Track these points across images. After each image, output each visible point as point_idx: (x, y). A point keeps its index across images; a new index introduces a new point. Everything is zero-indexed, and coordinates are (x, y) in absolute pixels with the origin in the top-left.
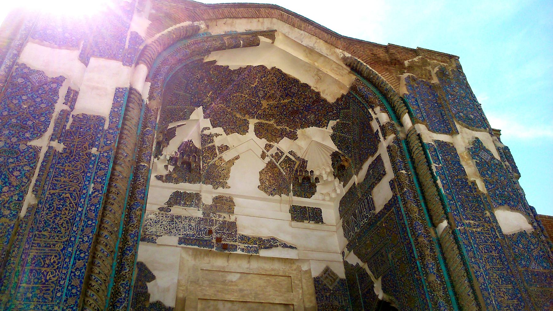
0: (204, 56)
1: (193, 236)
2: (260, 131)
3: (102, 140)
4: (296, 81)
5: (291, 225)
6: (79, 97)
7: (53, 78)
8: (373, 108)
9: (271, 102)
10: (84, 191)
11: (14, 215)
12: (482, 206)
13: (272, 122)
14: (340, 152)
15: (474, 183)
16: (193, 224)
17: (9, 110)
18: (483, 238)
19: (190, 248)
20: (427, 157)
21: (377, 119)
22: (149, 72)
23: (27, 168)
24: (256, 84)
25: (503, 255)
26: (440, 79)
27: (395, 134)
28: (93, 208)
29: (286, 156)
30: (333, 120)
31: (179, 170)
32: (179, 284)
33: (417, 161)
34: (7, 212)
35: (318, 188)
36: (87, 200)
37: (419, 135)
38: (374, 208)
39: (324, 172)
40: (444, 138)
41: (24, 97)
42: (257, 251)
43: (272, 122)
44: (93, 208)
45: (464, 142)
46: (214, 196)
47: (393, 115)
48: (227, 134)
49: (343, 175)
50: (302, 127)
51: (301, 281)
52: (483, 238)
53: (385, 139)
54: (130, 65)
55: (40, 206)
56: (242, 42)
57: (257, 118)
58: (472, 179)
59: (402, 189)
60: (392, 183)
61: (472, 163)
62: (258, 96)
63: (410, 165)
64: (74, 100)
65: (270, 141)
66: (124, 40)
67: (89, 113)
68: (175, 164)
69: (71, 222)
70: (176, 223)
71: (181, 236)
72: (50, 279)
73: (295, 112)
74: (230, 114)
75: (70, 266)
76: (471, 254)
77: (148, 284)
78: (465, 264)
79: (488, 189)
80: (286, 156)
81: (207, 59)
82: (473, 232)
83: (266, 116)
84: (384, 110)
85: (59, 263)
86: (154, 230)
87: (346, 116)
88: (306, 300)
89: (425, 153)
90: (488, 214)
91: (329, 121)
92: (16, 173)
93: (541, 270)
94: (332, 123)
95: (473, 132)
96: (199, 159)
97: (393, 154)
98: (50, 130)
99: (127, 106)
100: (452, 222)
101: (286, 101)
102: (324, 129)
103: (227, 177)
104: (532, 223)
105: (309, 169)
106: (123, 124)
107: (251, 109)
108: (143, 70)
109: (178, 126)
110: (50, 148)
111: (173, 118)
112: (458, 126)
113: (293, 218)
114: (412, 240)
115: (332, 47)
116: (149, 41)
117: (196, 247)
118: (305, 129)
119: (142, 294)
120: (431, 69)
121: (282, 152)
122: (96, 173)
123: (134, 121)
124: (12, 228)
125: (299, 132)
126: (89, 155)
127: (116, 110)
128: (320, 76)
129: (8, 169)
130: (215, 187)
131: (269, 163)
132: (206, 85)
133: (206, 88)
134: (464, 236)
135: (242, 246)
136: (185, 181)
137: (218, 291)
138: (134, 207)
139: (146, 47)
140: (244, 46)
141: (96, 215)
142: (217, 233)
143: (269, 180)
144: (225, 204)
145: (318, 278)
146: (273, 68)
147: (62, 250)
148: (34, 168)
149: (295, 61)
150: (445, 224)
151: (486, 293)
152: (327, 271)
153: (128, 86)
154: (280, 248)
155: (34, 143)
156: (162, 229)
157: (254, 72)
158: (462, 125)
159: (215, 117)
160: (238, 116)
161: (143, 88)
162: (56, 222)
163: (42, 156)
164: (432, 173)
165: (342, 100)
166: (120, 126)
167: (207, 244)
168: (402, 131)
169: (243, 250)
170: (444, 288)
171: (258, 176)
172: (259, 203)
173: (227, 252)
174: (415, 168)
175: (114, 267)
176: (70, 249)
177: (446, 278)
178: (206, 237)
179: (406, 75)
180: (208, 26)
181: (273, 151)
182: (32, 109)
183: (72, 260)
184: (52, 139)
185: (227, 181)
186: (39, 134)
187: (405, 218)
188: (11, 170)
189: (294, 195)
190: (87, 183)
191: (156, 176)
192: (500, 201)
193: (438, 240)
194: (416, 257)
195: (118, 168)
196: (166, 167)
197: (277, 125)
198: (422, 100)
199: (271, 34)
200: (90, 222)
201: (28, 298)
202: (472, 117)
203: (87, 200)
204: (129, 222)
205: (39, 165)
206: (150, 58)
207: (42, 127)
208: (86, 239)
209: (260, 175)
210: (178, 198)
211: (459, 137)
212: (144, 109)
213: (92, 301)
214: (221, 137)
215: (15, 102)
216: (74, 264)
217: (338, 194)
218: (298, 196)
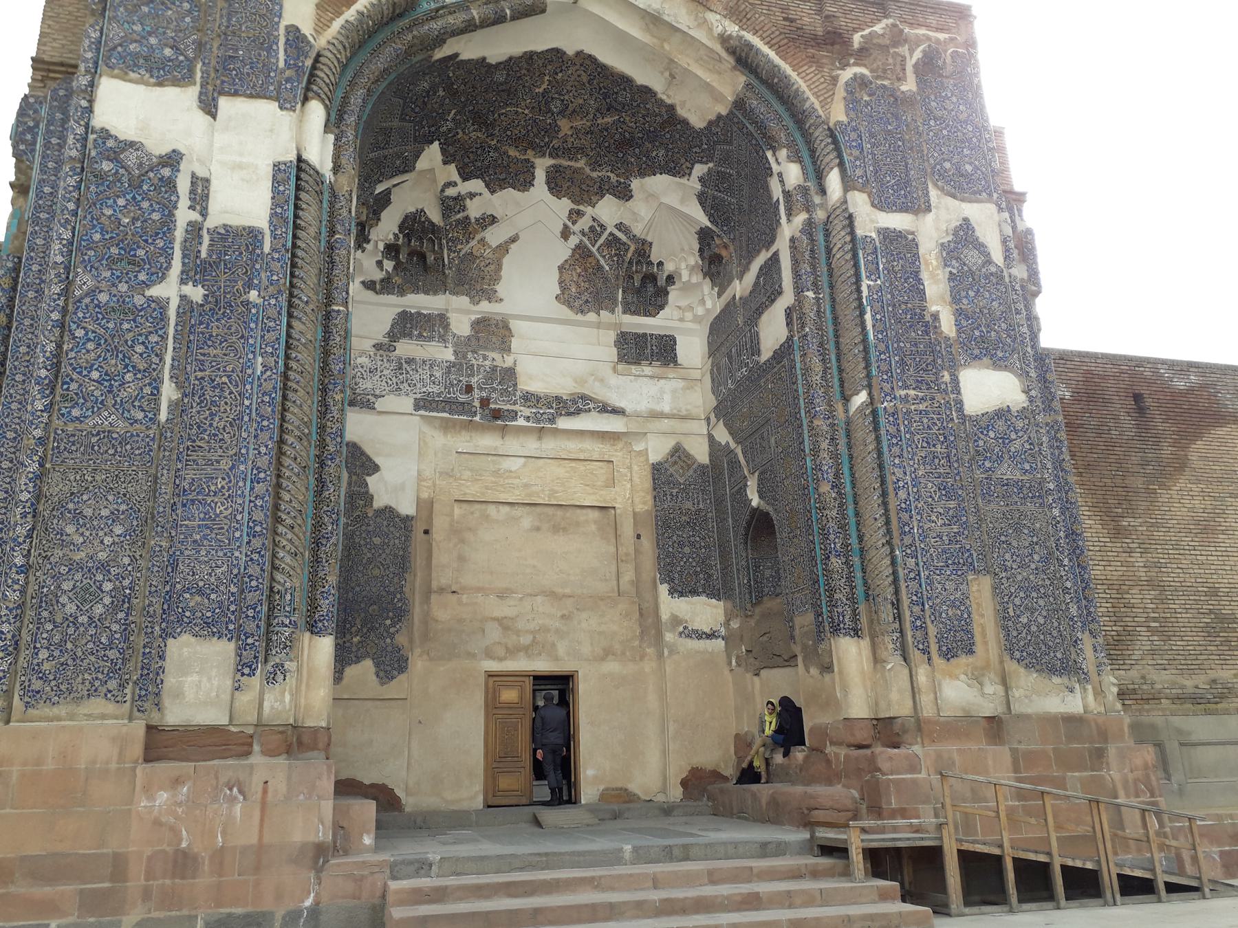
0: (433, 49)
1: (439, 395)
2: (556, 184)
3: (263, 275)
4: (626, 81)
5: (615, 370)
6: (212, 189)
7: (161, 157)
8: (774, 149)
9: (578, 123)
10: (249, 371)
11: (151, 419)
12: (939, 361)
13: (581, 164)
14: (714, 228)
15: (936, 317)
16: (438, 374)
17: (102, 229)
18: (925, 421)
19: (436, 417)
20: (856, 266)
21: (780, 175)
22: (328, 115)
23: (154, 338)
24: (544, 86)
25: (954, 451)
26: (921, 81)
27: (808, 211)
28: (267, 399)
30: (701, 162)
31: (405, 269)
32: (420, 478)
33: (836, 273)
34: (140, 415)
35: (671, 297)
36: (255, 386)
37: (850, 218)
38: (759, 353)
39: (683, 266)
40: (897, 221)
41: (121, 202)
42: (552, 420)
43: (581, 164)
44: (267, 399)
45: (937, 229)
46: (473, 317)
47: (810, 169)
48: (492, 192)
49: (719, 273)
50: (642, 174)
51: (630, 468)
52: (925, 421)
53: (789, 220)
54: (293, 109)
55: (186, 400)
56: (508, 12)
57: (551, 156)
58: (934, 308)
59: (803, 327)
60: (789, 313)
61: (942, 274)
62: (550, 111)
63: (824, 280)
65: (578, 203)
66: (275, 47)
67: (235, 221)
68: (396, 258)
69: (236, 423)
70: (408, 373)
71: (418, 396)
72: (221, 512)
73: (626, 143)
74: (496, 149)
75: (247, 492)
76: (896, 450)
77: (369, 479)
78: (881, 467)
79: (959, 331)
80: (611, 234)
81: (439, 54)
82: (908, 412)
83: (570, 153)
84: (796, 157)
85: (229, 488)
86: (369, 385)
87: (726, 159)
88: (637, 500)
89: (855, 256)
90: (947, 377)
91: (693, 165)
92: (139, 349)
93: (1018, 475)
94: (700, 169)
95: (964, 205)
97: (798, 257)
99: (297, 198)
100: (875, 393)
101: (609, 120)
102: (684, 181)
103: (496, 278)
104: (1026, 391)
105: (654, 258)
106: (295, 237)
107: (539, 137)
108: (316, 112)
109: (394, 186)
110: (183, 298)
111: (382, 174)
112: (933, 193)
113: (622, 358)
114: (805, 422)
115: (701, 8)
116: (321, 42)
118: (647, 179)
119: (359, 496)
120: (907, 54)
121: (602, 226)
122: (262, 337)
123: (312, 231)
124: (153, 439)
125: (635, 184)
127: (279, 210)
128: (674, 74)
129: (126, 341)
131: (579, 246)
132: (444, 98)
134: (891, 419)
135: (527, 412)
136: (416, 290)
137: (487, 488)
138: (331, 387)
139: (316, 60)
140: (513, 18)
141: (273, 411)
142: (481, 389)
144: (493, 332)
145: (660, 463)
146: (579, 54)
147: (231, 469)
148: (164, 338)
149: (622, 38)
150: (861, 398)
151: (905, 516)
152: (678, 452)
153: (292, 157)
154: (593, 413)
156: (384, 383)
157: (540, 62)
158: (942, 189)
159: (466, 160)
160: (512, 152)
161: (320, 152)
162: (215, 424)
164: (860, 299)
165: (718, 126)
166: (289, 244)
167: (464, 408)
168: (822, 206)
170: (841, 505)
172: (559, 329)
173: (499, 422)
174: (832, 287)
175: (311, 487)
176: (242, 467)
177: (848, 488)
178: (463, 398)
179: (846, 75)
181: (584, 223)
182: (139, 224)
183: (248, 483)
184: (183, 282)
185: (497, 288)
186: (160, 275)
187: (800, 382)
188: (130, 343)
189: (624, 312)
190: (251, 356)
191: (363, 283)
192: (977, 352)
193: (848, 423)
194: (807, 451)
195: (295, 323)
196: (380, 263)
197: (593, 170)
198: (872, 135)
200: (265, 423)
201: (195, 541)
202: (969, 168)
203: (255, 386)
204: (325, 413)
205: (171, 331)
206: (327, 85)
207: (162, 259)
208: (263, 450)
209: (561, 273)
210: (406, 325)
211: (930, 217)
212: (326, 196)
213: (285, 543)
214: (481, 199)
215: (109, 212)
216: (252, 489)
217: (708, 310)
218: (635, 313)
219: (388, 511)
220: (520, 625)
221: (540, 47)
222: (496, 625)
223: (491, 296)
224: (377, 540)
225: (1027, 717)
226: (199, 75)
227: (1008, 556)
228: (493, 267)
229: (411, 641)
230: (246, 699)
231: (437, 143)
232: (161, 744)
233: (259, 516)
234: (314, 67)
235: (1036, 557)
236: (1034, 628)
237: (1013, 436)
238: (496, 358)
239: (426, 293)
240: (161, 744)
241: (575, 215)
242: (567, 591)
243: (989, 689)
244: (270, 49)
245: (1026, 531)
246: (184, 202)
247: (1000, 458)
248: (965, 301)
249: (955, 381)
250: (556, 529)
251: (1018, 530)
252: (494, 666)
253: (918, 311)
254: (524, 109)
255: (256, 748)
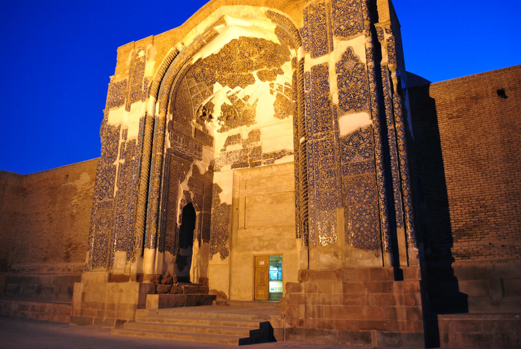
4: (256, 39)
9: (256, 56)
18: (324, 144)
29: (285, 87)
42: (273, 162)
43: (265, 68)
46: (249, 131)
50: (282, 64)
52: (324, 144)
64: (126, 135)
67: (131, 139)
74: (238, 75)
77: (220, 195)
80: (285, 87)
82: (317, 142)
96: (235, 112)
98: (119, 155)
107: (249, 66)
110: (120, 163)
117: (240, 168)
126: (132, 161)
130: (248, 126)
131: (277, 95)
133: (211, 72)
134: (310, 147)
135: (264, 161)
139: (151, 84)
143: (281, 108)
144: (255, 135)
154: (287, 156)
155: (114, 164)
160: (244, 74)
163: (117, 169)
167: (245, 165)
169: (265, 163)
171: (273, 108)
178: (244, 161)
180: (183, 44)
181: (276, 87)
192: (348, 108)
196: (219, 124)
199: (221, 21)
202: (352, 24)
210: (230, 140)
219: (225, 204)
220: (264, 238)
221: (228, 42)
222: (257, 239)
223: (252, 122)
224: (221, 214)
225: (353, 269)
226: (125, 103)
227: (353, 198)
228: (253, 112)
229: (231, 246)
230: (128, 266)
231: (217, 82)
232: (112, 278)
233: (132, 218)
234: (151, 86)
235: (367, 196)
236: (362, 229)
237: (362, 142)
238: (256, 144)
239: (234, 128)
240: (112, 278)
241: (272, 85)
242: (282, 224)
243: (340, 257)
244: (141, 87)
245: (363, 185)
246: (121, 137)
247: (354, 154)
248: (344, 86)
249: (337, 123)
250: (279, 202)
251: (359, 185)
252: (255, 253)
253: (326, 97)
254: (238, 61)
255: (130, 279)
